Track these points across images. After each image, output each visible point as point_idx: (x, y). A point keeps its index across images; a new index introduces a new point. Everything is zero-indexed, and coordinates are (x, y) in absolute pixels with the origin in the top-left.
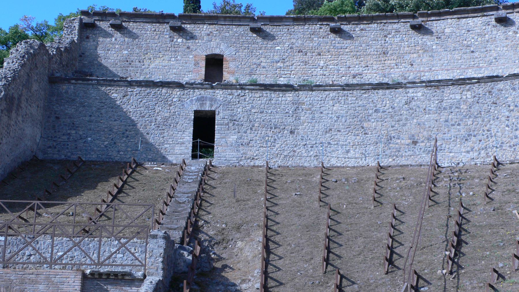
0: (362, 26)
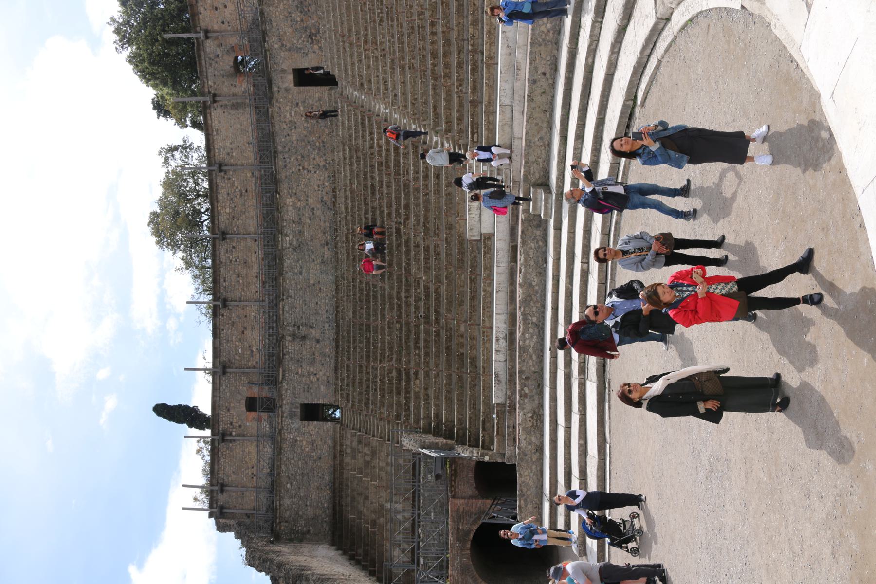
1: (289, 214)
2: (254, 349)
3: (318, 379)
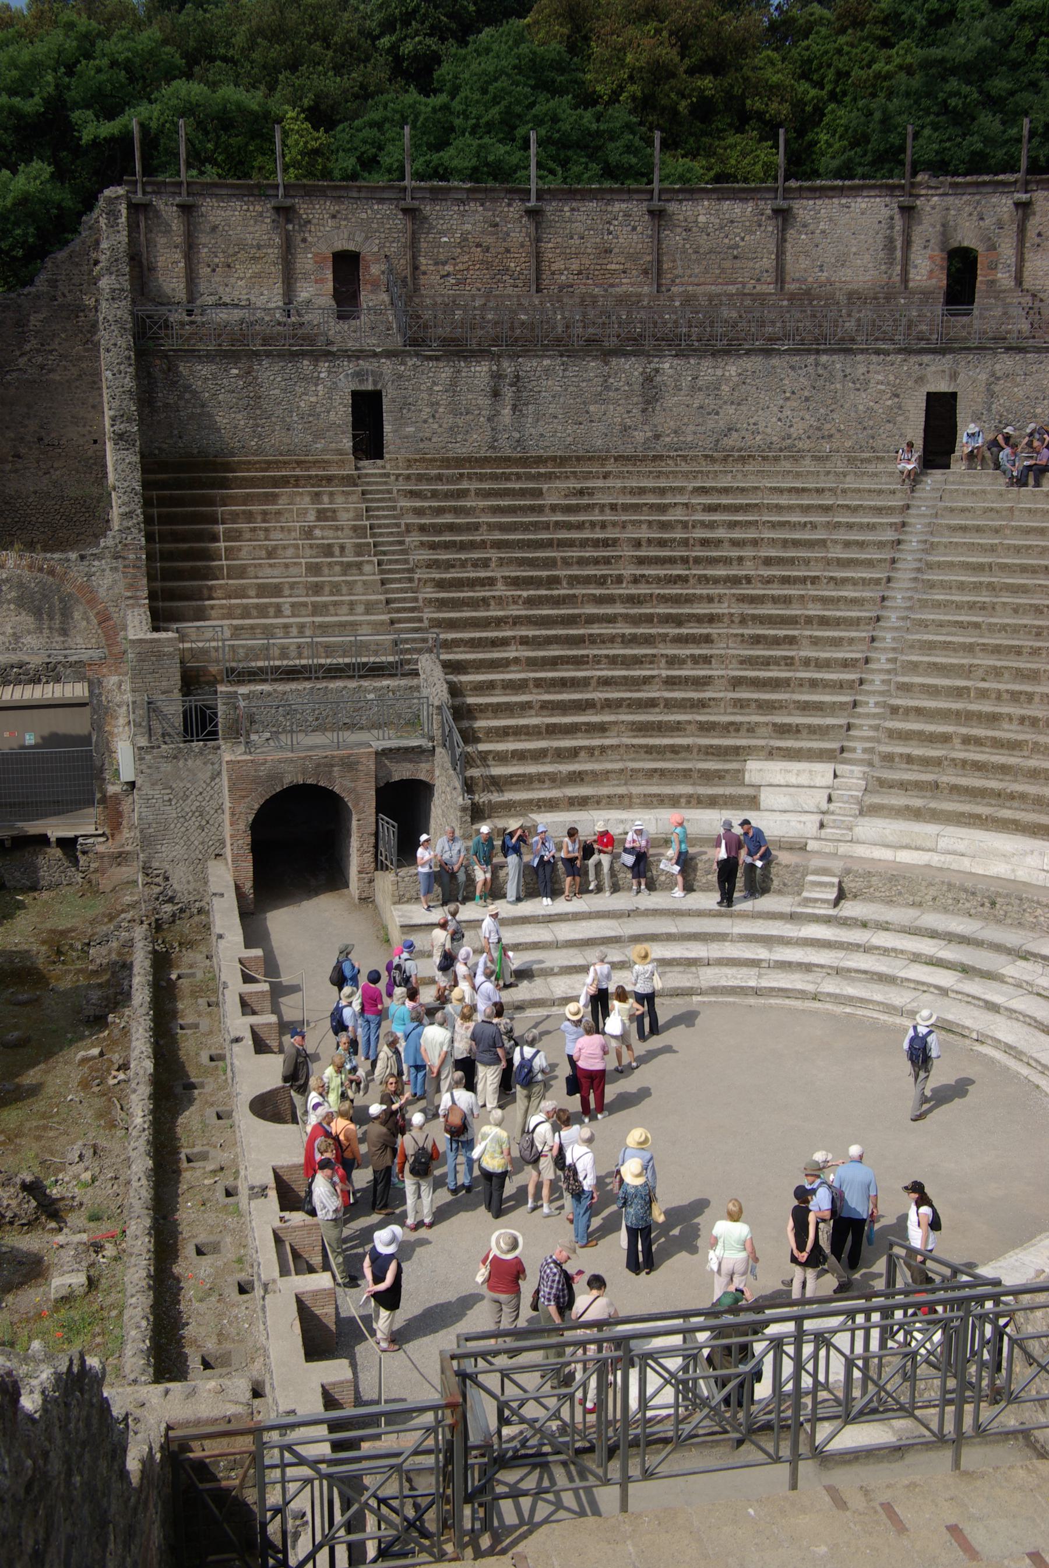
0: (574, 205)
1: (708, 370)
2: (449, 268)
3: (425, 422)
